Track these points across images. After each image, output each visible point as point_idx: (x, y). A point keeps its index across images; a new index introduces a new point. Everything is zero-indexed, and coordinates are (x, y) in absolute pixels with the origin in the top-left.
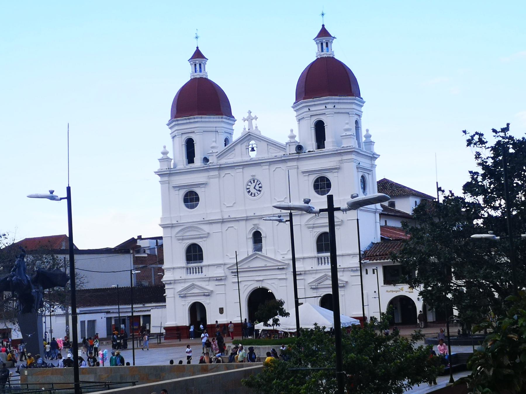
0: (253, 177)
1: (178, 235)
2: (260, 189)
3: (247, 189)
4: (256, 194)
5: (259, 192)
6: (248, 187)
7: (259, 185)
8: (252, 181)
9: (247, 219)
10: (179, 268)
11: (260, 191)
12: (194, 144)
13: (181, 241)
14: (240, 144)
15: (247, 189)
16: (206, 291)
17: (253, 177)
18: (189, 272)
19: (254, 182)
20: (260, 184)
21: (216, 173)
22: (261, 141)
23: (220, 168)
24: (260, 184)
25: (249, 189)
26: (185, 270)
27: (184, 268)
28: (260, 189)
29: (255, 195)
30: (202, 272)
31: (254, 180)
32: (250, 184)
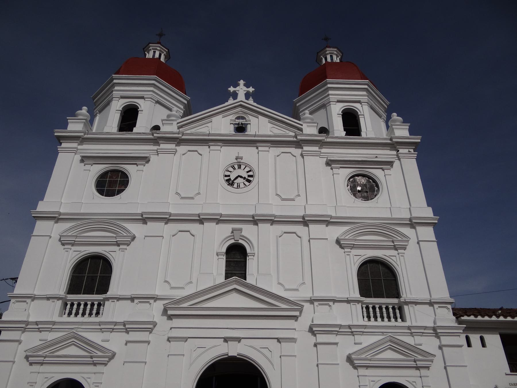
0: (239, 160)
1: (70, 234)
2: (250, 178)
3: (226, 176)
4: (242, 185)
5: (247, 183)
6: (228, 173)
7: (248, 172)
8: (236, 167)
9: (219, 220)
10: (48, 299)
11: (249, 181)
12: (138, 112)
13: (70, 246)
14: (221, 116)
15: (226, 176)
16: (100, 354)
17: (239, 160)
18: (67, 311)
19: (240, 167)
20: (250, 171)
21: (172, 146)
22: (260, 117)
23: (179, 141)
24: (250, 171)
25: (229, 176)
26: (59, 304)
27: (59, 299)
28: (250, 178)
29: (238, 186)
30: (98, 313)
31: (240, 165)
32: (231, 169)
